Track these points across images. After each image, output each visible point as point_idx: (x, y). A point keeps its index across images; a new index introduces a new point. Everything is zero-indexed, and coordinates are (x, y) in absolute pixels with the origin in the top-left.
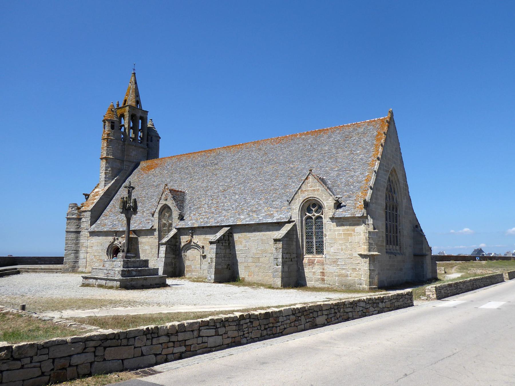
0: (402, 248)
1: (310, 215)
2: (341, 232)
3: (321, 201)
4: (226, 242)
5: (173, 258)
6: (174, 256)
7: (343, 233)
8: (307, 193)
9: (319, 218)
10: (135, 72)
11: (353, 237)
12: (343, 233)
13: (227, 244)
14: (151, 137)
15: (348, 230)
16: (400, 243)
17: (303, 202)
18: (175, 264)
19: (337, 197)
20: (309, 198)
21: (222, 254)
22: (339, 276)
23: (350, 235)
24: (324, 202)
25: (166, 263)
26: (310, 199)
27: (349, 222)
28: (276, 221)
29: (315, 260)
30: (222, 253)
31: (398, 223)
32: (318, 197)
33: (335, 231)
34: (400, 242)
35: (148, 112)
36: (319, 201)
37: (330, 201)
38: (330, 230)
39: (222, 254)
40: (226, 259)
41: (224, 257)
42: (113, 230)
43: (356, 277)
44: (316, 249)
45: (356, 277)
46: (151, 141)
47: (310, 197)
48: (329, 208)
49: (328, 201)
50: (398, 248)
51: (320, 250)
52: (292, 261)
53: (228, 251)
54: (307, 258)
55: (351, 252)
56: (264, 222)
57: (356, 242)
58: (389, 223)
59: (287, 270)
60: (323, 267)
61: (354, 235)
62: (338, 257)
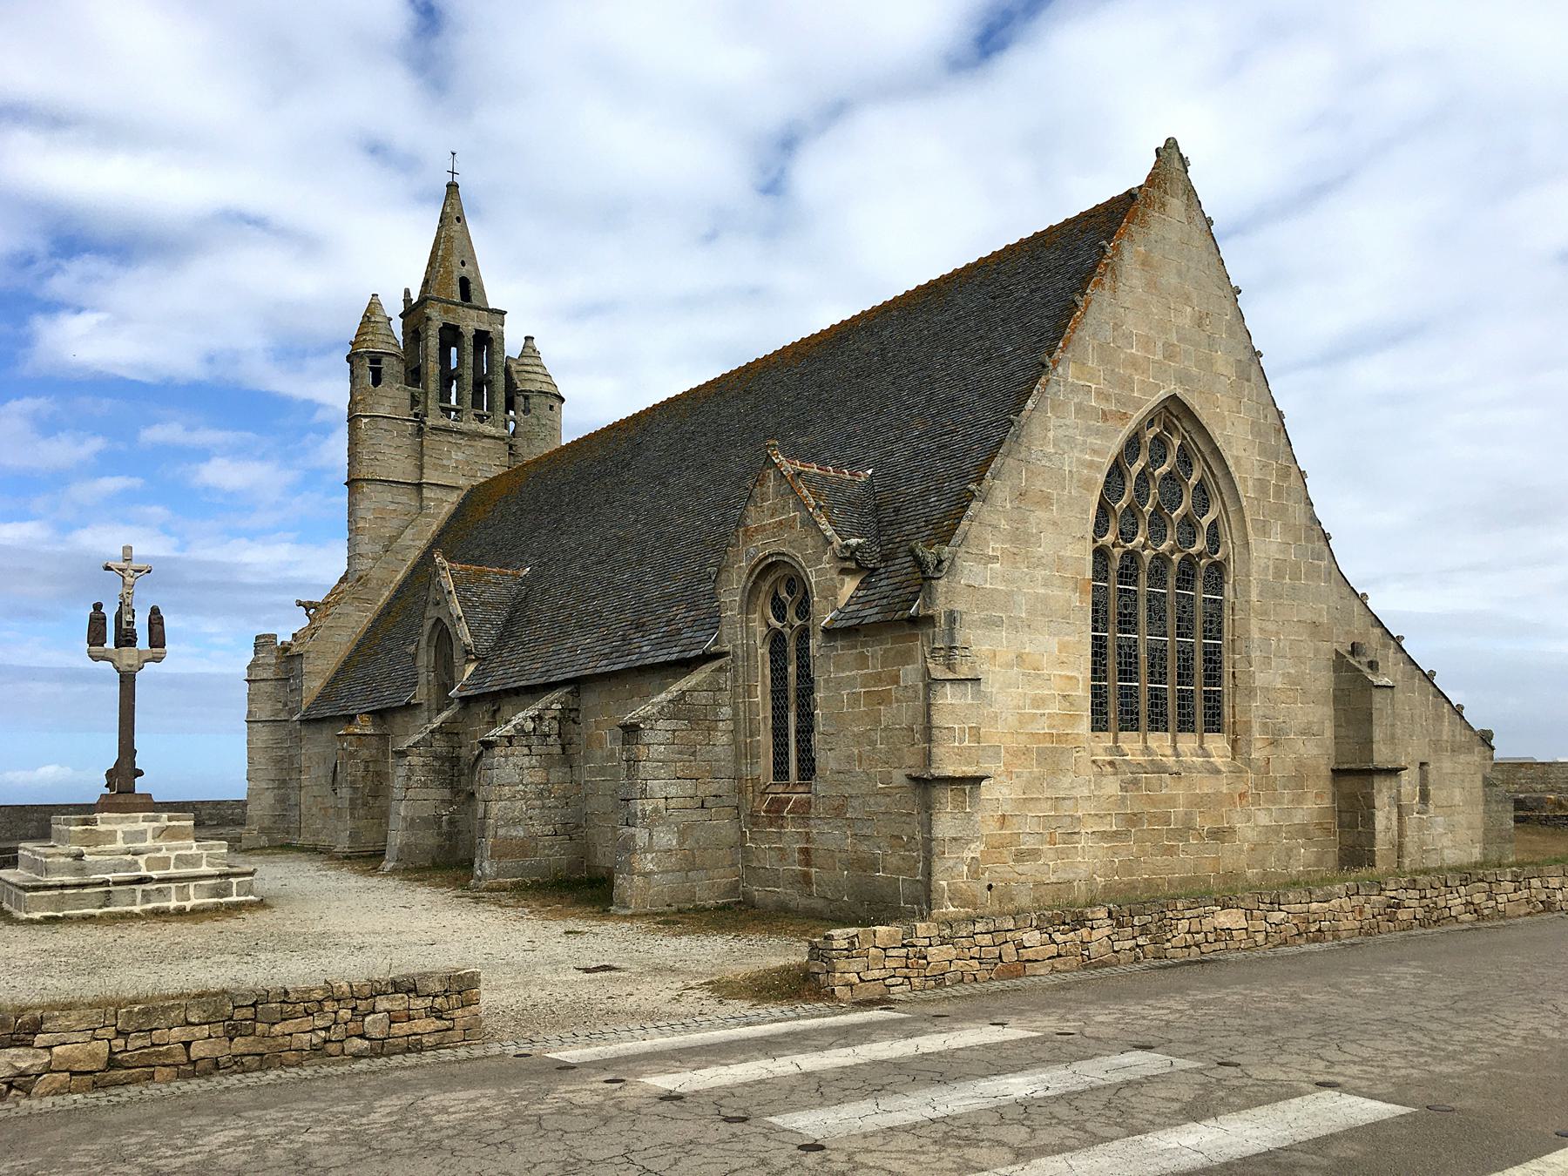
0: (1240, 743)
1: (778, 625)
2: (858, 690)
3: (801, 565)
4: (551, 740)
5: (443, 801)
6: (446, 794)
7: (863, 690)
8: (763, 540)
9: (804, 635)
10: (457, 179)
11: (894, 705)
12: (863, 690)
13: (557, 750)
14: (526, 398)
15: (878, 679)
16: (1234, 723)
17: (750, 575)
18: (451, 822)
19: (847, 546)
20: (766, 558)
21: (526, 785)
22: (849, 865)
23: (883, 698)
24: (808, 570)
25: (412, 819)
26: (770, 560)
27: (883, 647)
28: (674, 657)
29: (789, 800)
30: (527, 779)
31: (1227, 636)
32: (792, 551)
33: (840, 684)
34: (1234, 717)
35: (503, 313)
36: (797, 566)
37: (828, 566)
38: (826, 681)
39: (526, 785)
40: (551, 802)
41: (540, 795)
42: (341, 713)
43: (899, 870)
44: (799, 760)
45: (899, 870)
46: (527, 411)
47: (771, 555)
48: (824, 594)
49: (823, 566)
50: (1217, 744)
51: (808, 769)
52: (702, 807)
53: (556, 774)
54: (771, 796)
55: (886, 769)
56: (649, 661)
57: (904, 725)
58: (1112, 635)
59: (674, 842)
60: (807, 830)
61: (897, 700)
62: (848, 791)
